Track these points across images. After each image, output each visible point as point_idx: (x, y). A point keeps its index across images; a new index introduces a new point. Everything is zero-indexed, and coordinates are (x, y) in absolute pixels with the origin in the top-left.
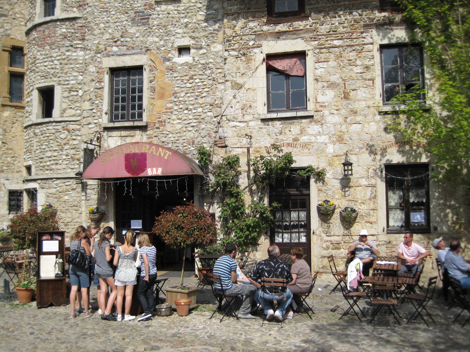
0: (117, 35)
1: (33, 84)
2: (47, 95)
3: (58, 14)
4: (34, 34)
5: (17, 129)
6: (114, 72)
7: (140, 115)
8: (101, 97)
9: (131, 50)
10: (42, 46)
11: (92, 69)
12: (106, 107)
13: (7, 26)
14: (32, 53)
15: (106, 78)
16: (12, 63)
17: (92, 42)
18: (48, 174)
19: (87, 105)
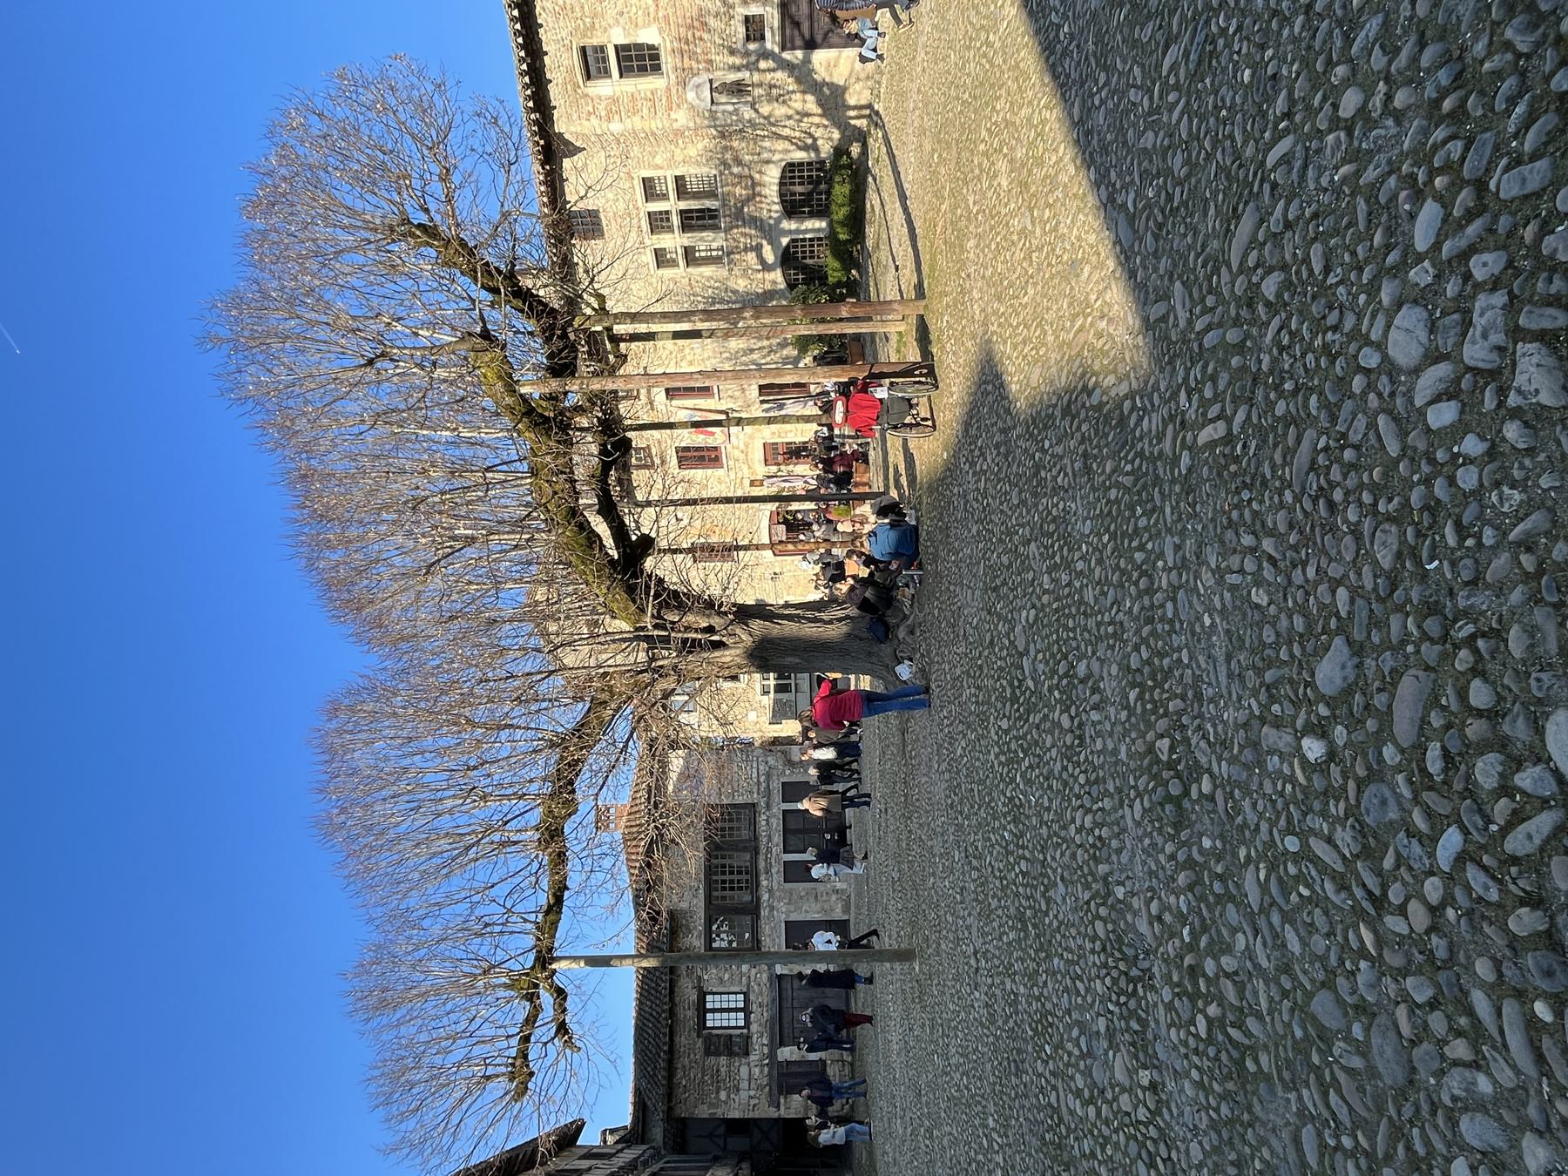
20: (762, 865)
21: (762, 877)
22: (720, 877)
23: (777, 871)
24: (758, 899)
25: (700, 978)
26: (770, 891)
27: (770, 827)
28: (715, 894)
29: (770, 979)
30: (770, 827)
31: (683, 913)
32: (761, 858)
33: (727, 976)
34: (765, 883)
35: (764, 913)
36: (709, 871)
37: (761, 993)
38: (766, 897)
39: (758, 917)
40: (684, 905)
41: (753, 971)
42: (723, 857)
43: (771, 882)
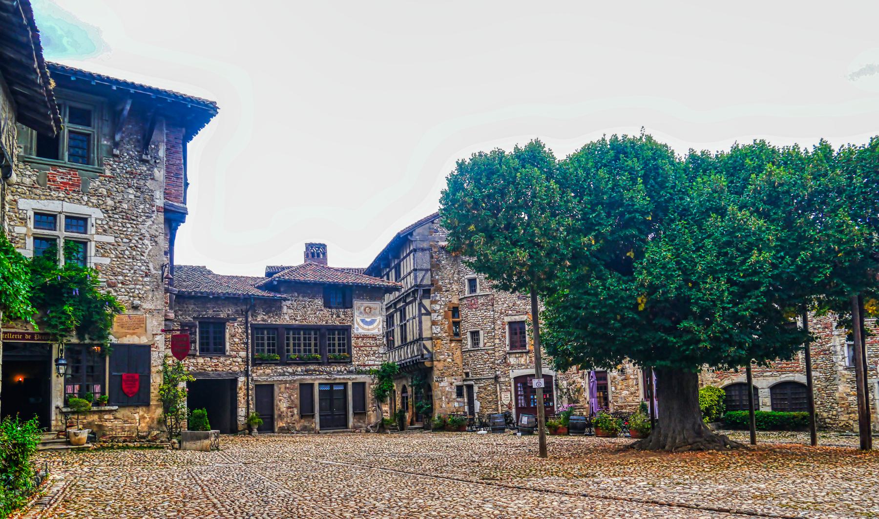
0: (511, 305)
1: (467, 328)
2: (475, 334)
3: (478, 292)
4: (465, 302)
5: (458, 352)
6: (510, 323)
7: (525, 346)
8: (505, 337)
9: (518, 313)
10: (471, 309)
11: (499, 322)
12: (507, 342)
13: (450, 297)
14: (464, 312)
15: (507, 327)
16: (453, 316)
17: (498, 307)
18: (479, 376)
19: (497, 341)
20: (312, 367)
21: (304, 368)
22: (337, 337)
23: (308, 379)
24: (289, 365)
25: (235, 320)
26: (293, 374)
27: (338, 374)
28: (291, 333)
29: (234, 372)
30: (338, 374)
31: (280, 308)
32: (316, 367)
33: (237, 340)
34: (299, 369)
35: (279, 369)
36: (307, 329)
37: (224, 365)
38: (290, 370)
39: (277, 364)
40: (285, 310)
41: (240, 360)
42: (315, 339)
43: (296, 374)
